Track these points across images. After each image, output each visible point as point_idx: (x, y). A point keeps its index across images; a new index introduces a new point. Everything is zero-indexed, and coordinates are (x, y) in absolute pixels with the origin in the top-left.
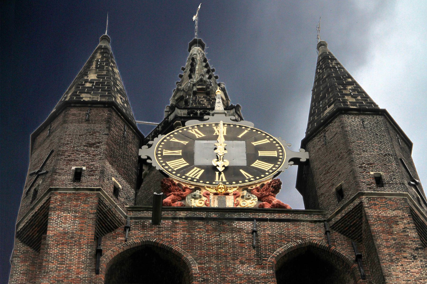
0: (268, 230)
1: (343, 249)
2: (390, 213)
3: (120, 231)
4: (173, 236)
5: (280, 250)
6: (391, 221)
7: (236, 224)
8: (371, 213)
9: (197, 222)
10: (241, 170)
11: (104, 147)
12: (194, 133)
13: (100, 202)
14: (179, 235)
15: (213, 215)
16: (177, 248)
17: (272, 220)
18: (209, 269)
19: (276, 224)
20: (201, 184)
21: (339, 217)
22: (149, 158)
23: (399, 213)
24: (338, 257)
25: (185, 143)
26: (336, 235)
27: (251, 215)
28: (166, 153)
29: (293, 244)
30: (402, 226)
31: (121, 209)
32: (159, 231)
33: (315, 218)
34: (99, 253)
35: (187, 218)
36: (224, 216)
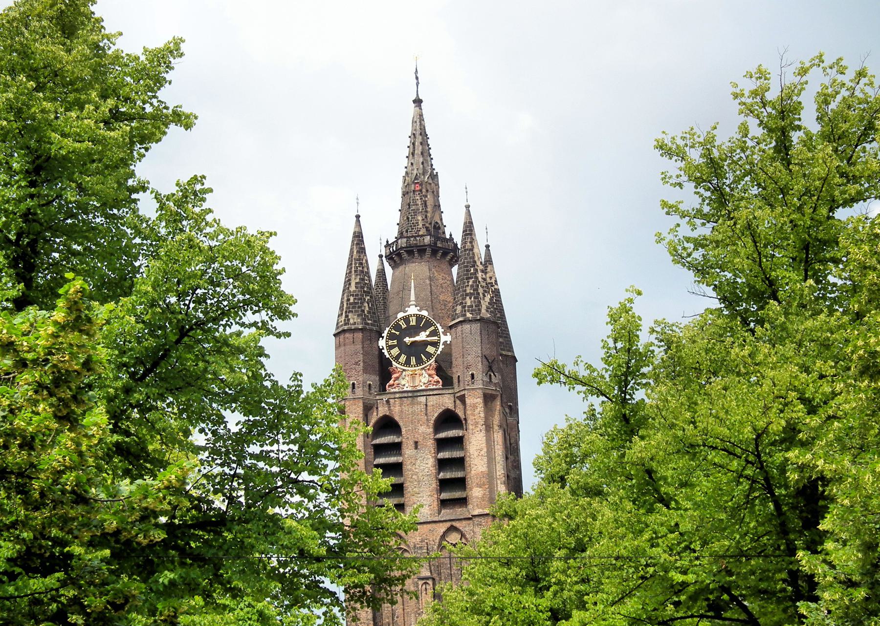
0: (432, 400)
1: (460, 412)
2: (476, 401)
5: (436, 415)
6: (474, 407)
15: (410, 395)
16: (397, 418)
19: (434, 397)
25: (398, 333)
26: (458, 402)
27: (425, 393)
29: (441, 410)
33: (450, 391)
36: (415, 394)
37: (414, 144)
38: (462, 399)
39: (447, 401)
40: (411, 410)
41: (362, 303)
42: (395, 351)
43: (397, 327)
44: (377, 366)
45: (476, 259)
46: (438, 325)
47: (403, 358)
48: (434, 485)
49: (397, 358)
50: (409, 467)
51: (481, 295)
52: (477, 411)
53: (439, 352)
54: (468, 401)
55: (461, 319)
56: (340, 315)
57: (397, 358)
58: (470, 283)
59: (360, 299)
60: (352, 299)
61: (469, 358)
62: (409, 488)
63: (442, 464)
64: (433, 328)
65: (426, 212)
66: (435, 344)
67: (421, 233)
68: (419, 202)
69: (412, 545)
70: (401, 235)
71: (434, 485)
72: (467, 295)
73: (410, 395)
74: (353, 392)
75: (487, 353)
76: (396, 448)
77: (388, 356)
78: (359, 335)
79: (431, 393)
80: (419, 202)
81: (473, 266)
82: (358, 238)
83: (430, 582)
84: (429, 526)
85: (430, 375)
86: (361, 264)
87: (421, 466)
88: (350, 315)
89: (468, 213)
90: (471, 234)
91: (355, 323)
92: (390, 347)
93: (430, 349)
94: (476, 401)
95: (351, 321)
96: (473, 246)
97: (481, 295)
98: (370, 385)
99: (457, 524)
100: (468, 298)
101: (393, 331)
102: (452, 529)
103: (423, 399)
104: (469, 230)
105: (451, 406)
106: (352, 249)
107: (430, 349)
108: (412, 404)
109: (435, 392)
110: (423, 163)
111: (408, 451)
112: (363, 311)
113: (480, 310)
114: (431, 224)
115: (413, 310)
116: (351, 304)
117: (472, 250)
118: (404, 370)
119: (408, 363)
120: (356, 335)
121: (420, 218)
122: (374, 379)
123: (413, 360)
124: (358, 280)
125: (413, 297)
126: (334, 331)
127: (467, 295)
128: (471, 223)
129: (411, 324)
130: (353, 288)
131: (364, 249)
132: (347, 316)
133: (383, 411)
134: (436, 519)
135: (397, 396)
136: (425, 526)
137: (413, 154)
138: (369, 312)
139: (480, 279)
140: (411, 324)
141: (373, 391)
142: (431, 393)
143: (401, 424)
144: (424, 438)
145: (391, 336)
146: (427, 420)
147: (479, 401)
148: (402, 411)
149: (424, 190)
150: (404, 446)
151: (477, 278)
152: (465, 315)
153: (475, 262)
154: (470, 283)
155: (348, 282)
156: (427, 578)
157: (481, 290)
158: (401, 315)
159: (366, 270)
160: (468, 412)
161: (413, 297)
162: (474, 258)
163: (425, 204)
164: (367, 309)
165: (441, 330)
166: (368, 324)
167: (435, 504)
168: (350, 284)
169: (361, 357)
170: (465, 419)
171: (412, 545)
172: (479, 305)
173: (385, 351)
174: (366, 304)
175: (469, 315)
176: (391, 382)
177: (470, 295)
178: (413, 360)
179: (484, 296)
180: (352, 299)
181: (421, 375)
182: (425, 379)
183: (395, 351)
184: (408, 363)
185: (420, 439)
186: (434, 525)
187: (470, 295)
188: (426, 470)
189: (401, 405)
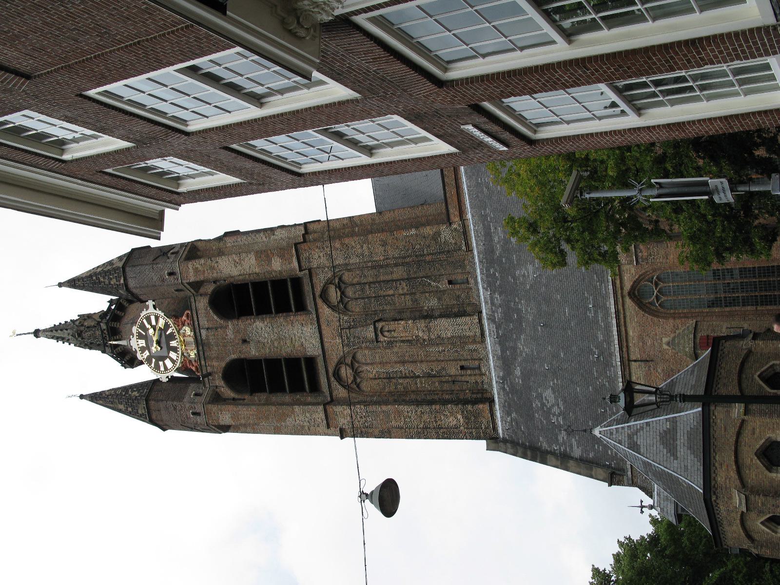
0: (204, 322)
1: (210, 288)
2: (191, 270)
4: (217, 366)
5: (215, 317)
6: (196, 270)
7: (204, 337)
8: (192, 279)
9: (206, 355)
10: (167, 333)
11: (175, 403)
12: (146, 356)
13: (209, 403)
14: (215, 364)
15: (201, 348)
16: (223, 364)
17: (198, 321)
18: (233, 350)
19: (200, 319)
20: (180, 353)
21: (192, 291)
22: (168, 377)
23: (190, 266)
24: (213, 291)
25: (154, 360)
26: (202, 291)
28: (162, 369)
29: (211, 311)
30: (198, 266)
31: (206, 392)
32: (215, 373)
33: (192, 300)
34: (234, 399)
35: (205, 360)
36: (199, 343)
38: (196, 286)
39: (202, 304)
40: (216, 348)
48: (282, 320)
50: (267, 351)
52: (200, 268)
53: (162, 314)
60: (130, 409)
61: (155, 278)
69: (346, 349)
73: (201, 348)
78: (152, 403)
79: (196, 323)
83: (380, 325)
84: (323, 327)
92: (166, 368)
98: (196, 395)
101: (153, 365)
102: (324, 295)
103: (204, 332)
108: (209, 344)
109: (195, 319)
117: (82, 278)
118: (183, 354)
120: (152, 408)
127: (110, 283)
129: (144, 345)
133: (219, 382)
134: (315, 316)
135: (203, 362)
136: (324, 332)
140: (144, 345)
141: (201, 391)
142: (196, 323)
143: (228, 359)
148: (217, 358)
152: (122, 284)
156: (375, 329)
167: (301, 317)
169: (169, 403)
171: (346, 349)
180: (130, 409)
181: (184, 336)
183: (168, 363)
185: (240, 336)
186: (322, 320)
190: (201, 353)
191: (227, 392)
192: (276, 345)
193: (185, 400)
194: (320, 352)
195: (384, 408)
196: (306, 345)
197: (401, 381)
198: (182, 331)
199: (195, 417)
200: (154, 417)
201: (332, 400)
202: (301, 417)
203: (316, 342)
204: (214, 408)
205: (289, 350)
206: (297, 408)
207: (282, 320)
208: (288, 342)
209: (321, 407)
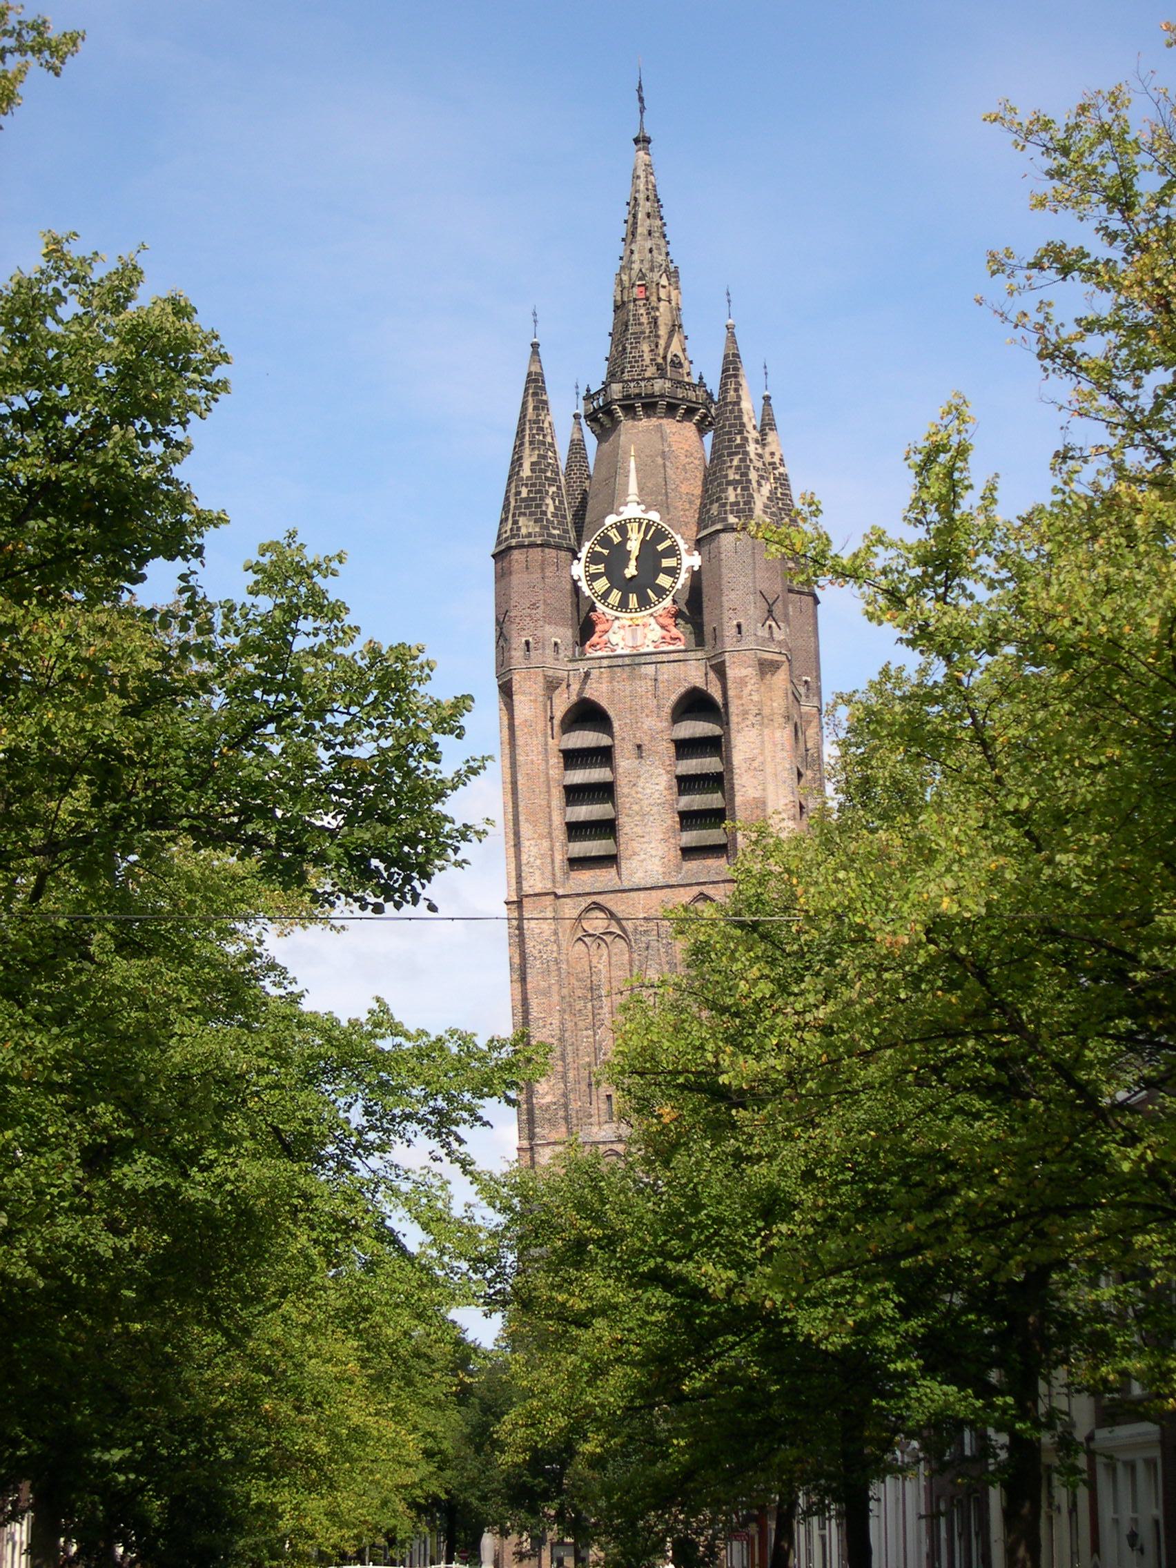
0: (667, 672)
1: (715, 693)
2: (744, 672)
3: (564, 686)
4: (598, 691)
6: (742, 682)
13: (545, 677)
15: (627, 661)
16: (604, 703)
25: (606, 552)
26: (712, 675)
27: (654, 658)
29: (682, 690)
31: (561, 667)
36: (635, 660)
37: (635, 216)
38: (720, 670)
39: (694, 674)
41: (542, 499)
42: (602, 584)
43: (605, 541)
44: (569, 610)
45: (745, 419)
46: (678, 538)
47: (615, 596)
48: (670, 822)
49: (605, 596)
51: (755, 485)
52: (746, 691)
53: (679, 586)
54: (731, 673)
55: (719, 527)
56: (503, 521)
57: (605, 596)
58: (735, 463)
59: (539, 492)
61: (733, 595)
62: (627, 826)
63: (686, 783)
64: (667, 543)
65: (658, 336)
66: (672, 572)
67: (648, 374)
68: (644, 320)
70: (612, 376)
71: (673, 820)
72: (729, 483)
74: (527, 658)
75: (763, 586)
76: (604, 755)
77: (588, 593)
78: (536, 554)
79: (665, 658)
80: (644, 320)
81: (741, 432)
82: (535, 383)
85: (663, 627)
86: (541, 429)
87: (648, 788)
88: (522, 521)
89: (732, 338)
90: (736, 376)
91: (529, 535)
92: (593, 578)
93: (664, 580)
94: (744, 672)
95: (524, 531)
96: (739, 397)
97: (755, 485)
99: (709, 890)
100: (731, 488)
102: (704, 897)
103: (650, 669)
104: (731, 367)
105: (699, 683)
106: (524, 404)
107: (664, 580)
108: (632, 678)
110: (651, 251)
111: (624, 761)
112: (545, 513)
113: (751, 510)
114: (665, 358)
115: (631, 510)
116: (523, 500)
117: (738, 403)
119: (623, 605)
121: (645, 347)
122: (563, 634)
123: (633, 600)
124: (534, 459)
125: (633, 487)
126: (492, 549)
127: (729, 483)
128: (737, 356)
130: (526, 472)
131: (545, 402)
132: (515, 522)
134: (673, 881)
135: (605, 663)
136: (653, 893)
137: (633, 234)
138: (555, 515)
139: (752, 456)
142: (665, 658)
143: (611, 713)
144: (653, 738)
145: (594, 558)
146: (658, 707)
147: (750, 672)
149: (654, 298)
150: (617, 753)
151: (746, 453)
152: (725, 519)
153: (743, 425)
154: (735, 463)
155: (517, 462)
157: (753, 476)
158: (611, 520)
159: (549, 439)
160: (731, 693)
161: (633, 487)
162: (740, 417)
163: (655, 322)
164: (551, 509)
165: (683, 546)
166: (553, 536)
168: (521, 465)
170: (726, 705)
172: (749, 501)
173: (583, 584)
174: (549, 501)
175: (732, 519)
176: (594, 639)
177: (734, 483)
178: (633, 600)
179: (760, 485)
180: (524, 492)
182: (656, 633)
183: (602, 584)
184: (623, 605)
185: (645, 741)
187: (734, 483)
188: (657, 795)
189: (612, 680)
190: (620, 661)
191: (562, 703)
192: (636, 807)
193: (547, 627)
194: (626, 885)
195: (555, 988)
196: (634, 863)
197: (589, 1005)
198: (652, 620)
199: (523, 646)
200: (516, 555)
201: (557, 897)
202: (534, 850)
203: (638, 879)
204: (538, 687)
205: (626, 829)
206: (546, 844)
207: (670, 822)
208: (638, 830)
209: (549, 886)
